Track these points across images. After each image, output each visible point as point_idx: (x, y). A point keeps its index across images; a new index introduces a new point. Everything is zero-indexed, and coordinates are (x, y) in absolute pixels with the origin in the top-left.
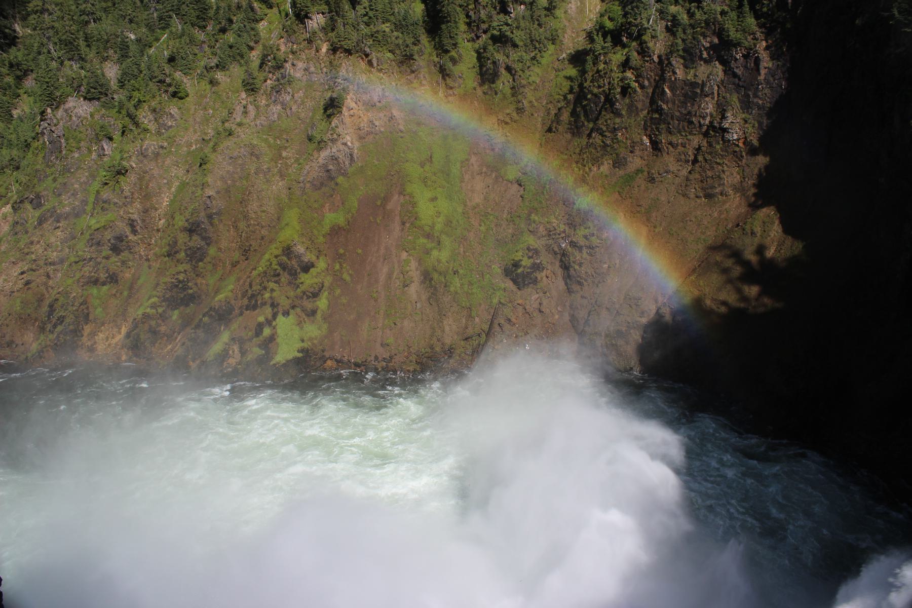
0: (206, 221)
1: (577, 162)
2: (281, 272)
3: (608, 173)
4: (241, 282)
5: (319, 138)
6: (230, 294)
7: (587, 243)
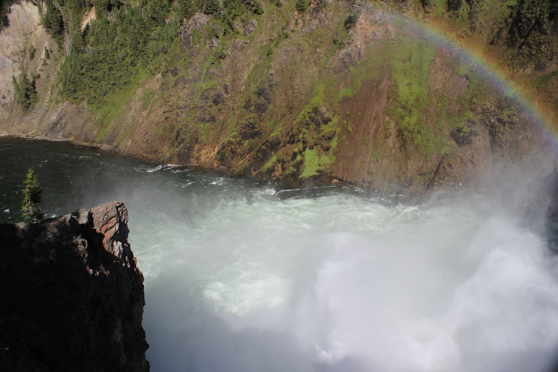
0: (268, 88)
1: (509, 66)
2: (311, 123)
3: (530, 73)
4: (286, 126)
5: (340, 42)
6: (279, 133)
7: (509, 121)
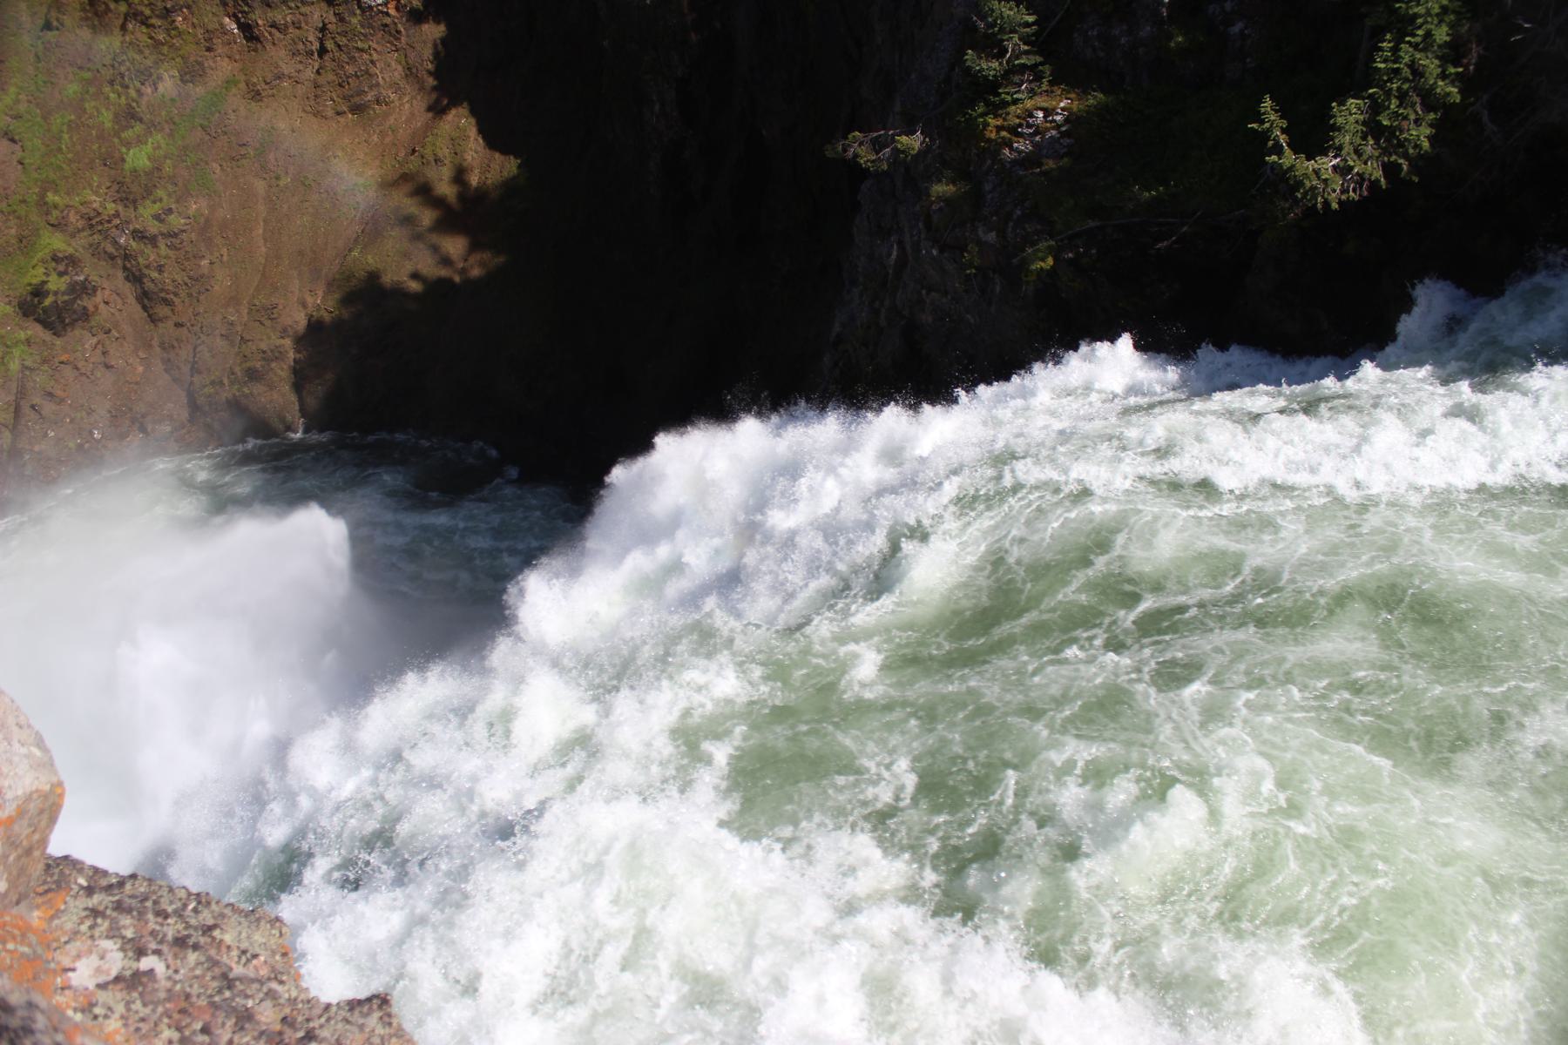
1: (111, 83)
